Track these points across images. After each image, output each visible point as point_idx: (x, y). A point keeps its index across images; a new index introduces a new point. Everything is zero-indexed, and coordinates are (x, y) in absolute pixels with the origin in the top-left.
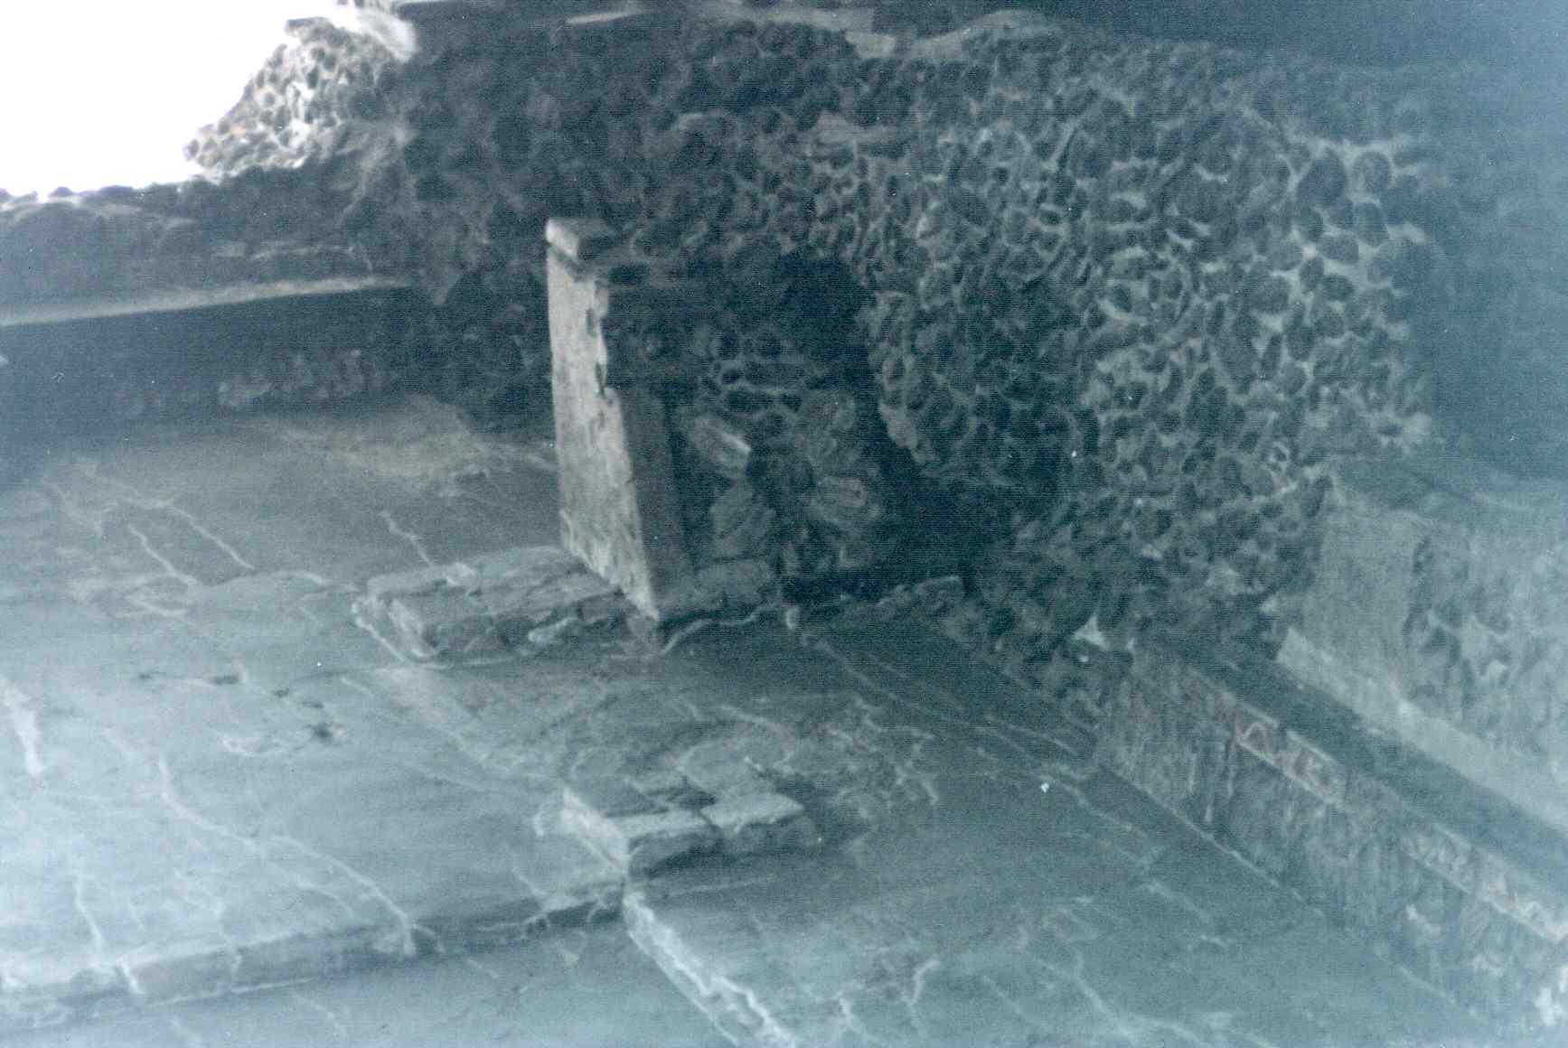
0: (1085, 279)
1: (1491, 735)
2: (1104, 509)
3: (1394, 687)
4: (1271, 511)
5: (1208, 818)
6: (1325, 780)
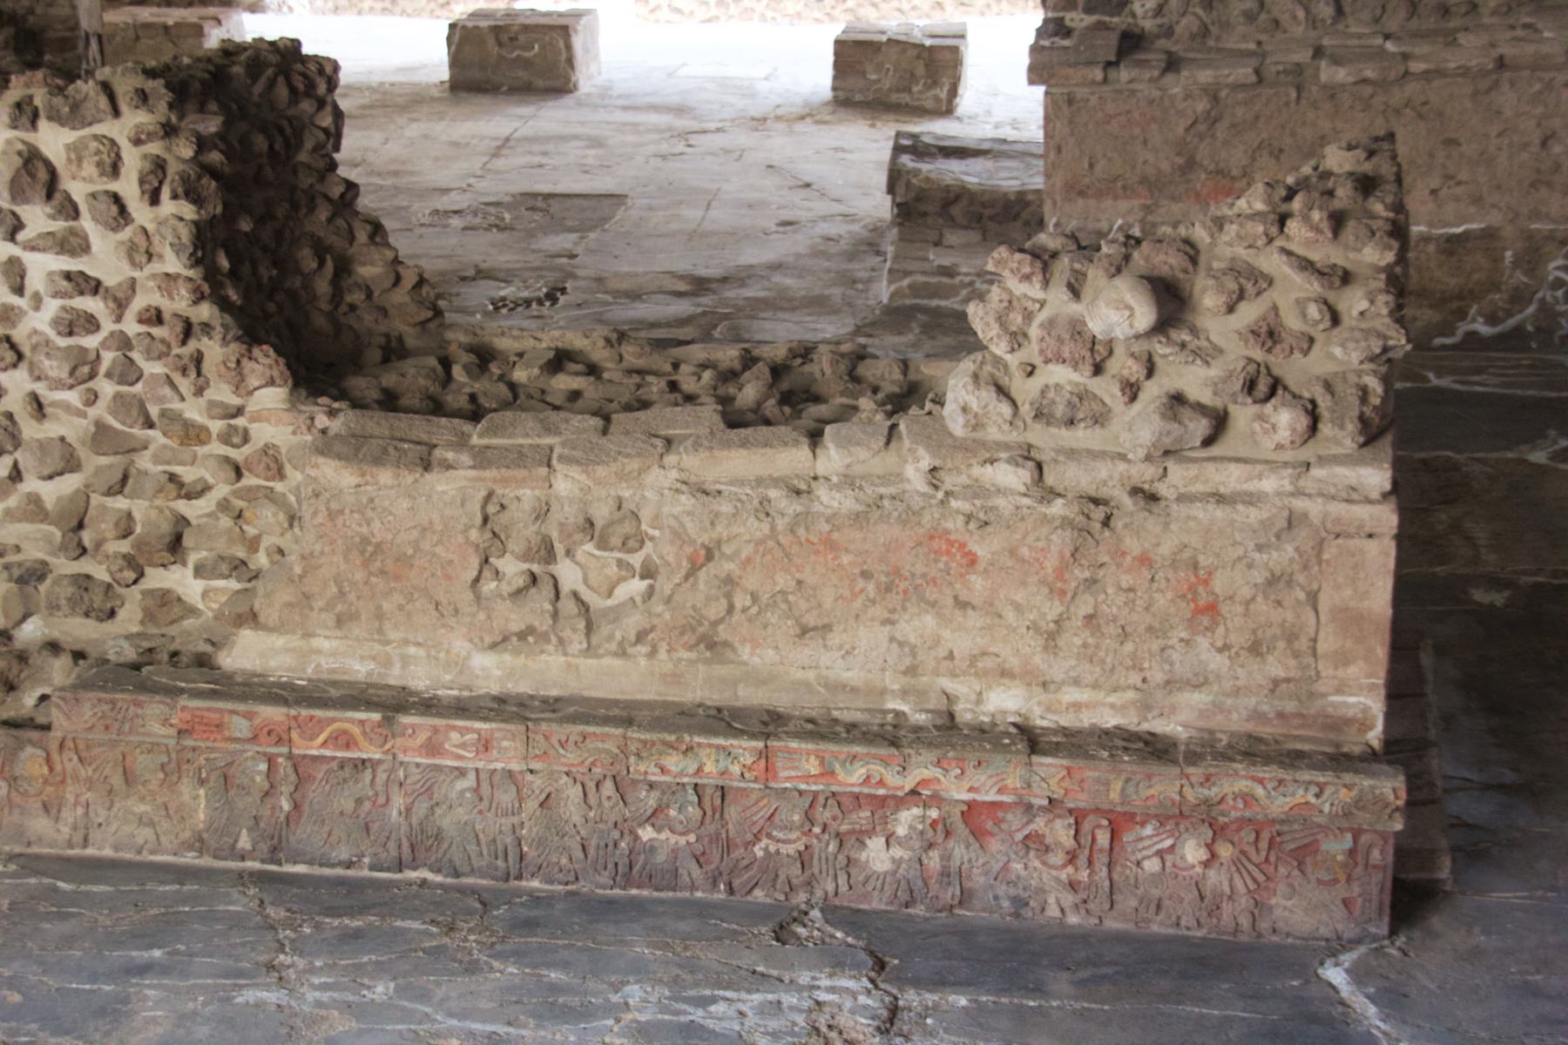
1: (643, 649)
3: (460, 645)
6: (485, 745)
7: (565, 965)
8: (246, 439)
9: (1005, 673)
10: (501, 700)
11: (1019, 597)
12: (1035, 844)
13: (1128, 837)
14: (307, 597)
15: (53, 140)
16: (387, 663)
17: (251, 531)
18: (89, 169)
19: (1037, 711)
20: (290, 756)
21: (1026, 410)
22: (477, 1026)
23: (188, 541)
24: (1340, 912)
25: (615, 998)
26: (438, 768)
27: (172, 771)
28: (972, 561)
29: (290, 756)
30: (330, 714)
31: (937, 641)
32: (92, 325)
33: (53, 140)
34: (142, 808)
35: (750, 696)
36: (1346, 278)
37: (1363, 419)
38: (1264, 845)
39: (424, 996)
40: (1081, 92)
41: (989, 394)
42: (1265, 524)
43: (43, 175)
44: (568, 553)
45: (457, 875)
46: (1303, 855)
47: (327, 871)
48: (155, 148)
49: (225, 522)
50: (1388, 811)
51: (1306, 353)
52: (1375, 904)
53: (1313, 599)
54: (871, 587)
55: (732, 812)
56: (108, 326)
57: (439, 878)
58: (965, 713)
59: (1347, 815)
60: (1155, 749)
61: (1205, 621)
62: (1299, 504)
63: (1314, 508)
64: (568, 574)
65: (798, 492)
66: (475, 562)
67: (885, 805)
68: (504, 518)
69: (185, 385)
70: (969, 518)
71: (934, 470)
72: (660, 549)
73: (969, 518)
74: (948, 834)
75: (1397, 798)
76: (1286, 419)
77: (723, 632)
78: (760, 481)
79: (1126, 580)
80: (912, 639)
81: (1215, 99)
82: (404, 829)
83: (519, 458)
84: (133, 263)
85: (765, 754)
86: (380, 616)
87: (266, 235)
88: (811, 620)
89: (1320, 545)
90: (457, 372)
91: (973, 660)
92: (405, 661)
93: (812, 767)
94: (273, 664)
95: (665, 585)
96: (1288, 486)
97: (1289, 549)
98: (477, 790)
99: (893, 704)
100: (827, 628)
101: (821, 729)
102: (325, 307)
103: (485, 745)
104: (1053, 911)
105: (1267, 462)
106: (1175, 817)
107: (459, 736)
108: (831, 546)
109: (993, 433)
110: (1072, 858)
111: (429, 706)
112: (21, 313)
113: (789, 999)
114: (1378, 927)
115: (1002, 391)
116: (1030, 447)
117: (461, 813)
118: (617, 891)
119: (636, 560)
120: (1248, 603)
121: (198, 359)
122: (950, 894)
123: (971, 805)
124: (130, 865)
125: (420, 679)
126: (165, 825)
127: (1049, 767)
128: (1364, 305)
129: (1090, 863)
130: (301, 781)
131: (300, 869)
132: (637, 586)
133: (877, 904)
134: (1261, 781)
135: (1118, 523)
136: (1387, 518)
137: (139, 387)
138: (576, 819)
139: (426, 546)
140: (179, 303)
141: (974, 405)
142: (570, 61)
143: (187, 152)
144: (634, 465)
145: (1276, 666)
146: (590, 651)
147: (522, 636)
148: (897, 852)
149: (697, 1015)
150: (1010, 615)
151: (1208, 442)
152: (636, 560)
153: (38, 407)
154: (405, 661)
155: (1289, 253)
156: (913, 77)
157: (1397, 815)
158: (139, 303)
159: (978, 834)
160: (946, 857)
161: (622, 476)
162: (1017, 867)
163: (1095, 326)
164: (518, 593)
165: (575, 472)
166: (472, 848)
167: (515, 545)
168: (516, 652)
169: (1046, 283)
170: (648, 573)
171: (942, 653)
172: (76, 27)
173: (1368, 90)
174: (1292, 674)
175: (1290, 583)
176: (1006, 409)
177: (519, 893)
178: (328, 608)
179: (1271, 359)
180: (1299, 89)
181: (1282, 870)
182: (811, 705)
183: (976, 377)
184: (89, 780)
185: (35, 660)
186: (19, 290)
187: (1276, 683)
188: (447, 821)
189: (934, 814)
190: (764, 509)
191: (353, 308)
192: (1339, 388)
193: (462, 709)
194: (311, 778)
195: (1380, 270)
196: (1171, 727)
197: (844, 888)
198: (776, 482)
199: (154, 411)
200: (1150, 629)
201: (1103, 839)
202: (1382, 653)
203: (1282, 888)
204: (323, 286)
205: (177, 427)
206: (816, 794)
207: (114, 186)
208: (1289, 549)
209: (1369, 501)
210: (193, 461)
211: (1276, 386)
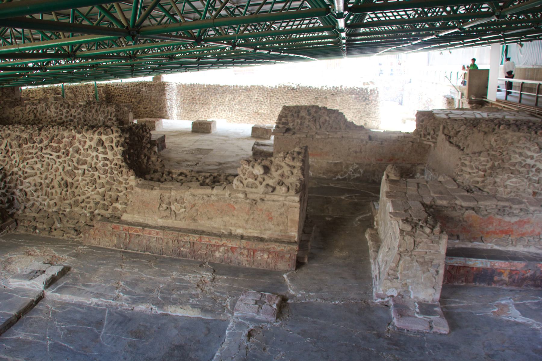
0: (18, 166)
1: (184, 220)
2: (33, 205)
3: (156, 218)
4: (88, 198)
5: (122, 246)
6: (157, 233)
7: (165, 268)
8: (128, 184)
9: (239, 227)
10: (162, 227)
11: (242, 215)
12: (241, 254)
13: (256, 253)
14: (134, 209)
15: (104, 137)
16: (145, 220)
17: (128, 198)
18: (108, 142)
19: (244, 233)
20: (129, 233)
21: (245, 185)
22: (149, 277)
23: (119, 199)
24: (288, 266)
25: (171, 274)
26: (151, 237)
27: (112, 234)
28: (235, 209)
29: (129, 233)
30: (135, 227)
31: (229, 221)
32: (107, 165)
33: (104, 137)
34: (107, 240)
35: (200, 228)
36: (294, 167)
37: (296, 190)
38: (276, 255)
39: (142, 271)
40: (279, 137)
41: (239, 183)
42: (280, 205)
43: (101, 142)
44: (173, 204)
45: (153, 253)
46: (282, 257)
47: (134, 252)
48: (118, 139)
49: (124, 196)
51: (288, 179)
53: (287, 217)
54: (219, 212)
55: (195, 246)
56: (109, 166)
57: (150, 254)
58: (233, 233)
59: (289, 251)
60: (261, 240)
61: (270, 220)
62: (285, 202)
63: (287, 203)
64: (173, 207)
65: (209, 196)
66: (159, 205)
67: (219, 246)
68: (163, 198)
69: (120, 175)
70: (234, 202)
71: (230, 194)
72: (187, 204)
73: (234, 202)
74: (228, 251)
76: (284, 189)
77: (196, 218)
78: (203, 194)
79: (258, 213)
80: (225, 220)
81: (300, 139)
82: (145, 246)
83: (167, 189)
84: (114, 156)
85: (200, 237)
86: (144, 212)
87: (136, 152)
88: (210, 217)
89: (288, 209)
90: (164, 175)
91: (235, 224)
92: (148, 220)
93: (207, 240)
94: (128, 219)
95: (187, 210)
96: (284, 199)
97: (283, 209)
98: (156, 240)
99: (222, 231)
100: (212, 218)
101: (210, 234)
102: (145, 164)
103: (157, 233)
104: (244, 265)
105: (281, 195)
106: (263, 250)
107: (154, 231)
108: (213, 205)
109: (240, 189)
110: (247, 256)
111: (150, 227)
112: (98, 163)
113: (198, 276)
115: (241, 182)
116: (245, 191)
117: (154, 244)
118: (177, 258)
119: (183, 206)
120: (277, 217)
121: (122, 171)
122: (229, 261)
123: (232, 247)
124: (105, 248)
125: (150, 223)
126: (110, 243)
127: (244, 241)
128: (297, 172)
129: (250, 257)
130: (130, 237)
131: (130, 251)
132: (183, 210)
133: (217, 262)
134: (276, 245)
135: (257, 204)
136: (298, 205)
137: (113, 175)
138: (171, 246)
139: (151, 202)
140: (119, 163)
141: (237, 184)
142: (210, 128)
143: (123, 140)
144: (184, 191)
145: (281, 228)
146: (176, 220)
147: (165, 217)
148: (220, 254)
149: (183, 277)
150: (240, 218)
151: (272, 192)
152: (183, 206)
153: (99, 177)
154: (148, 220)
155: (285, 163)
156: (264, 133)
158: (114, 162)
159: (233, 252)
160: (228, 255)
161: (182, 192)
162: (239, 257)
163: (254, 173)
164: (165, 210)
165: (174, 191)
166: (156, 250)
167: (165, 202)
168: (165, 219)
169: (249, 166)
170: (185, 208)
171: (230, 223)
172: (129, 121)
173: (323, 139)
174: (284, 229)
175: (283, 215)
176: (242, 185)
177: (162, 257)
178: (137, 211)
179: (283, 179)
180: (313, 138)
181: (279, 259)
182: (209, 230)
183: (238, 180)
184: (100, 235)
185: (96, 216)
186: (98, 160)
187: (281, 230)
188: (152, 245)
189: (226, 248)
190: (203, 199)
191: (150, 164)
192: (293, 184)
193: (155, 228)
194: (132, 237)
195: (299, 166)
196: (265, 236)
197: (212, 259)
198: (205, 194)
199: (115, 179)
200: (262, 221)
201: (252, 253)
202: (297, 226)
203: (279, 262)
204: (145, 161)
205: (118, 182)
206: (208, 244)
207: (112, 145)
208: (283, 209)
209: (296, 202)
210: (121, 187)
211: (283, 184)
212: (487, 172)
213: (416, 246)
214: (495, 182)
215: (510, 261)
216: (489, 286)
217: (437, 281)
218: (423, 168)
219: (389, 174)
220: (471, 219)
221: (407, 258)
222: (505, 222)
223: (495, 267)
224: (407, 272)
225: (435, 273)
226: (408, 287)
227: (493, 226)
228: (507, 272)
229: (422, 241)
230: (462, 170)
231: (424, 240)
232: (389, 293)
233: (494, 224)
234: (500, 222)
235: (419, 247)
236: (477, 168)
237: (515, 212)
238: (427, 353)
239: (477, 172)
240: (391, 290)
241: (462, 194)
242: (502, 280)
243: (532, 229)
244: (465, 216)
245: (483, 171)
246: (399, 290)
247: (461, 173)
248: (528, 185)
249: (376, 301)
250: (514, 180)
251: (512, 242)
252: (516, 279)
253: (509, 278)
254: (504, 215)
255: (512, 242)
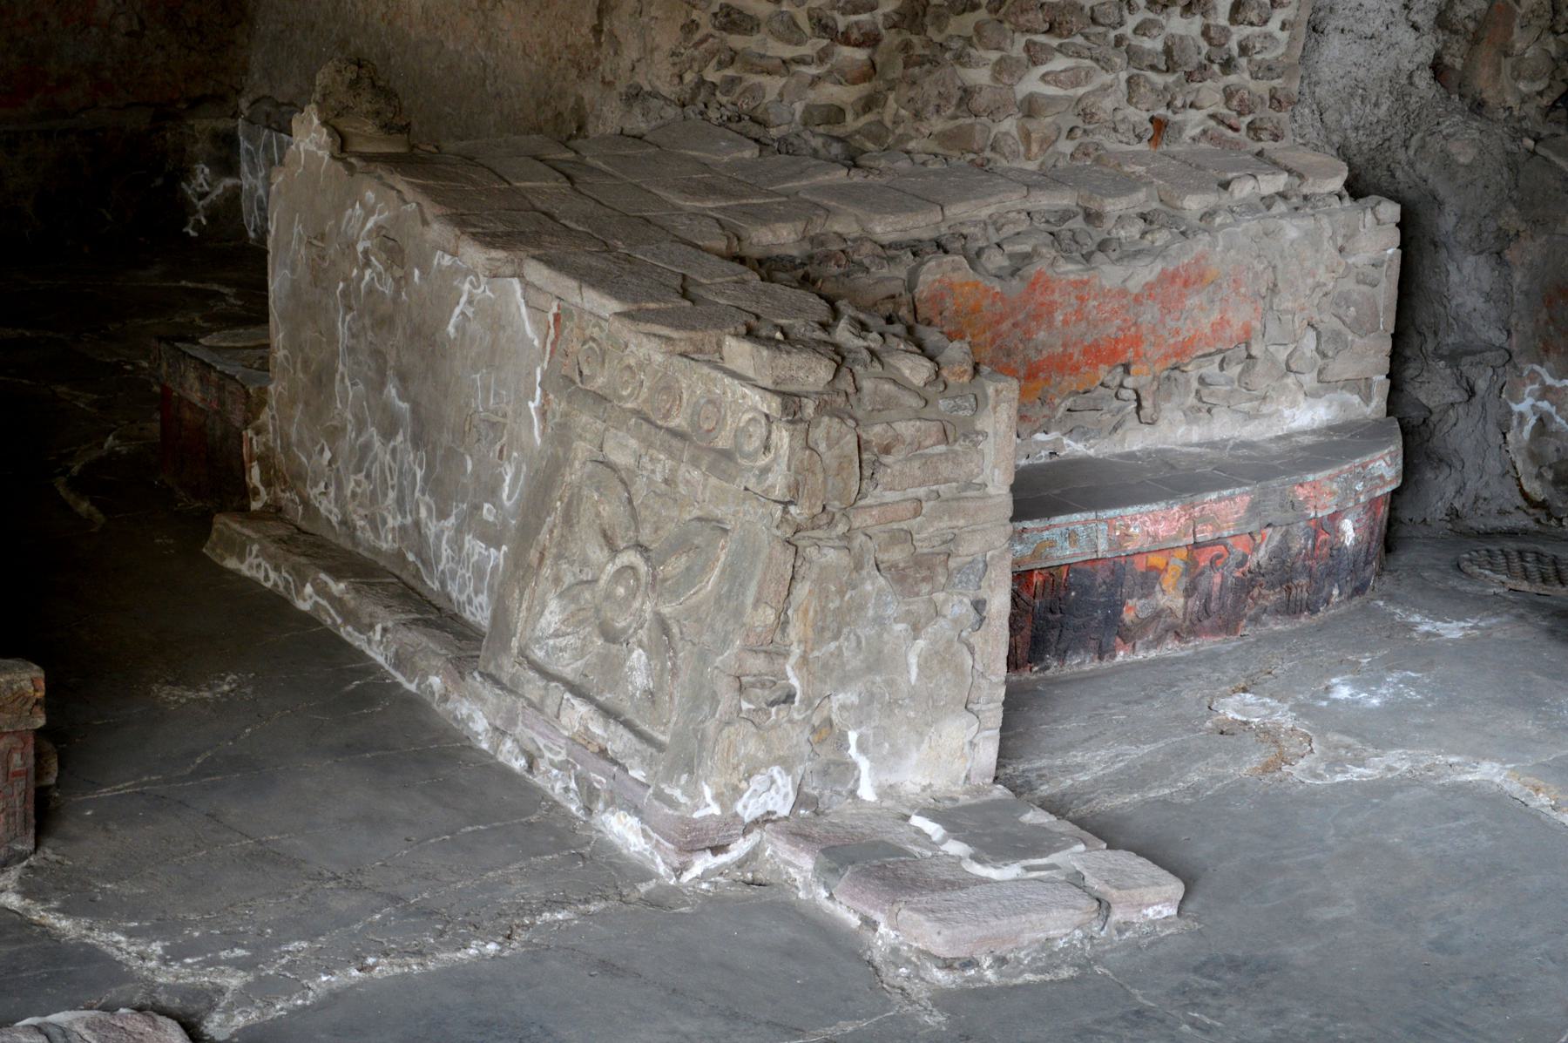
50: (29, 706)
52: (19, 818)
75: (36, 690)
114: (23, 843)
157: (38, 709)
212: (882, 45)
213: (867, 473)
214: (967, 93)
215: (1186, 496)
216: (1105, 664)
217: (979, 667)
218: (222, 125)
219: (343, 124)
220: (948, 302)
221: (831, 555)
222: (1104, 294)
223: (1131, 547)
224: (833, 645)
225: (973, 615)
226: (842, 743)
227: (1050, 324)
228: (1177, 563)
229: (898, 438)
230: (733, 57)
231: (906, 428)
232: (749, 808)
233: (1059, 317)
234: (1081, 299)
235: (883, 477)
236: (823, 26)
237: (1122, 233)
238: (1186, 1028)
239: (823, 56)
240: (758, 781)
241: (823, 179)
242: (1158, 614)
243: (1215, 316)
244: (922, 291)
245: (858, 45)
246: (800, 770)
247: (730, 72)
248: (1123, 86)
249: (687, 877)
250: (1059, 63)
251: (1138, 400)
252: (1216, 589)
253: (1189, 592)
254: (1087, 257)
255: (1138, 400)
